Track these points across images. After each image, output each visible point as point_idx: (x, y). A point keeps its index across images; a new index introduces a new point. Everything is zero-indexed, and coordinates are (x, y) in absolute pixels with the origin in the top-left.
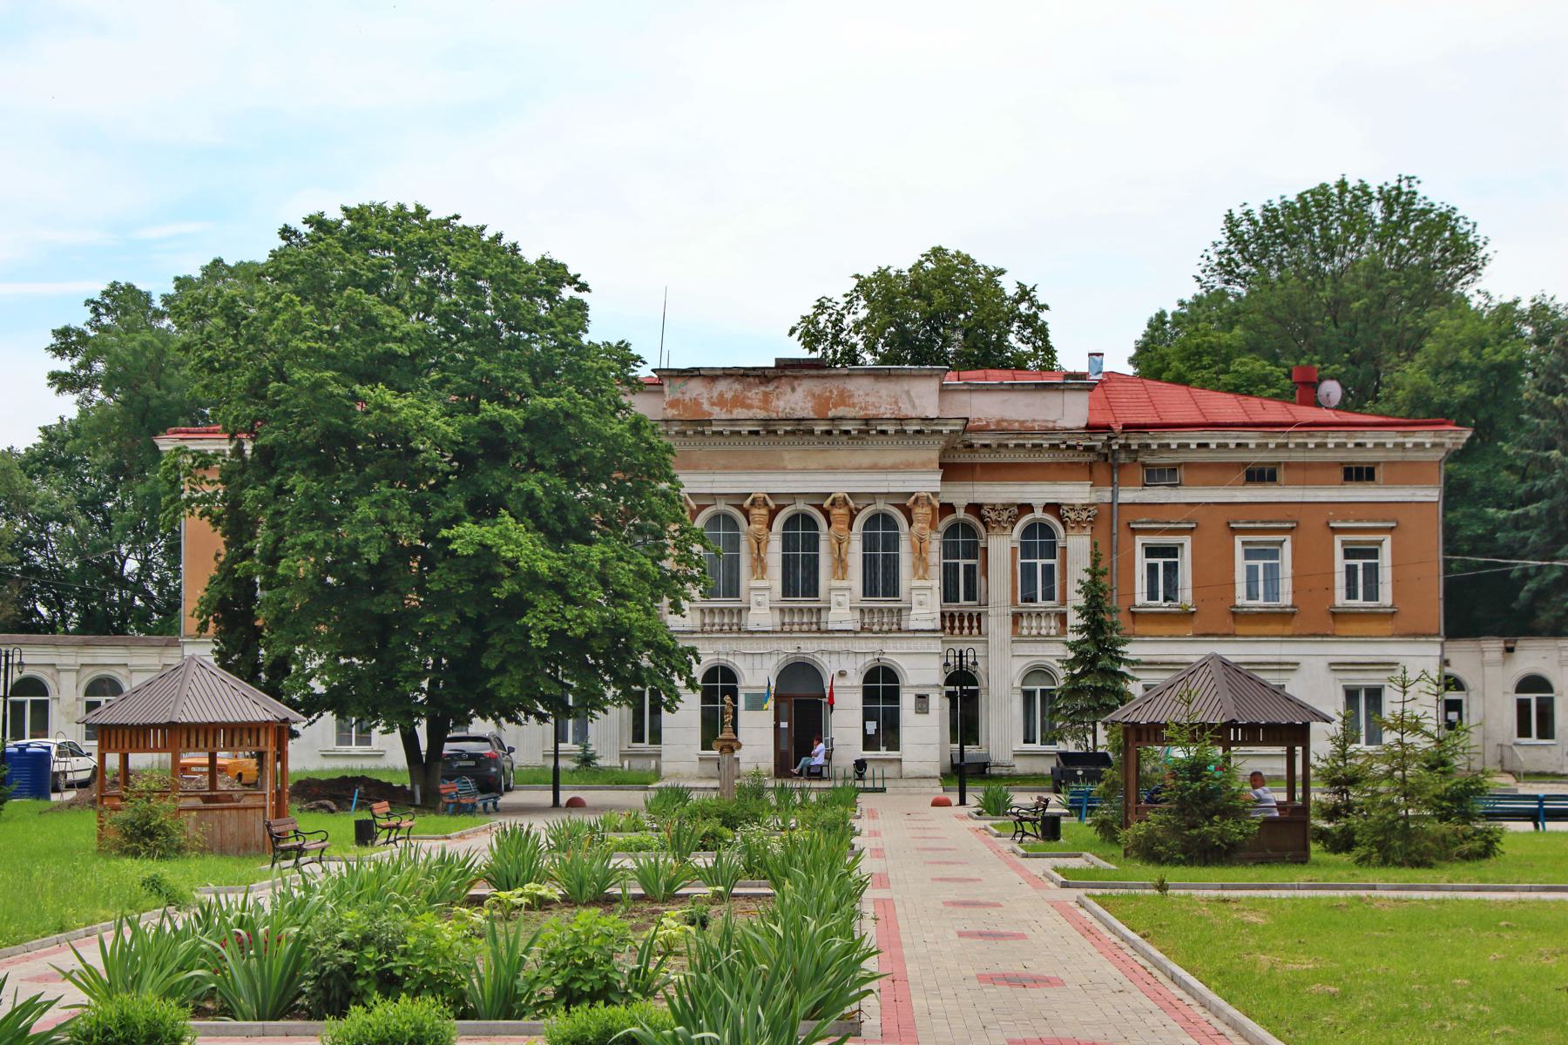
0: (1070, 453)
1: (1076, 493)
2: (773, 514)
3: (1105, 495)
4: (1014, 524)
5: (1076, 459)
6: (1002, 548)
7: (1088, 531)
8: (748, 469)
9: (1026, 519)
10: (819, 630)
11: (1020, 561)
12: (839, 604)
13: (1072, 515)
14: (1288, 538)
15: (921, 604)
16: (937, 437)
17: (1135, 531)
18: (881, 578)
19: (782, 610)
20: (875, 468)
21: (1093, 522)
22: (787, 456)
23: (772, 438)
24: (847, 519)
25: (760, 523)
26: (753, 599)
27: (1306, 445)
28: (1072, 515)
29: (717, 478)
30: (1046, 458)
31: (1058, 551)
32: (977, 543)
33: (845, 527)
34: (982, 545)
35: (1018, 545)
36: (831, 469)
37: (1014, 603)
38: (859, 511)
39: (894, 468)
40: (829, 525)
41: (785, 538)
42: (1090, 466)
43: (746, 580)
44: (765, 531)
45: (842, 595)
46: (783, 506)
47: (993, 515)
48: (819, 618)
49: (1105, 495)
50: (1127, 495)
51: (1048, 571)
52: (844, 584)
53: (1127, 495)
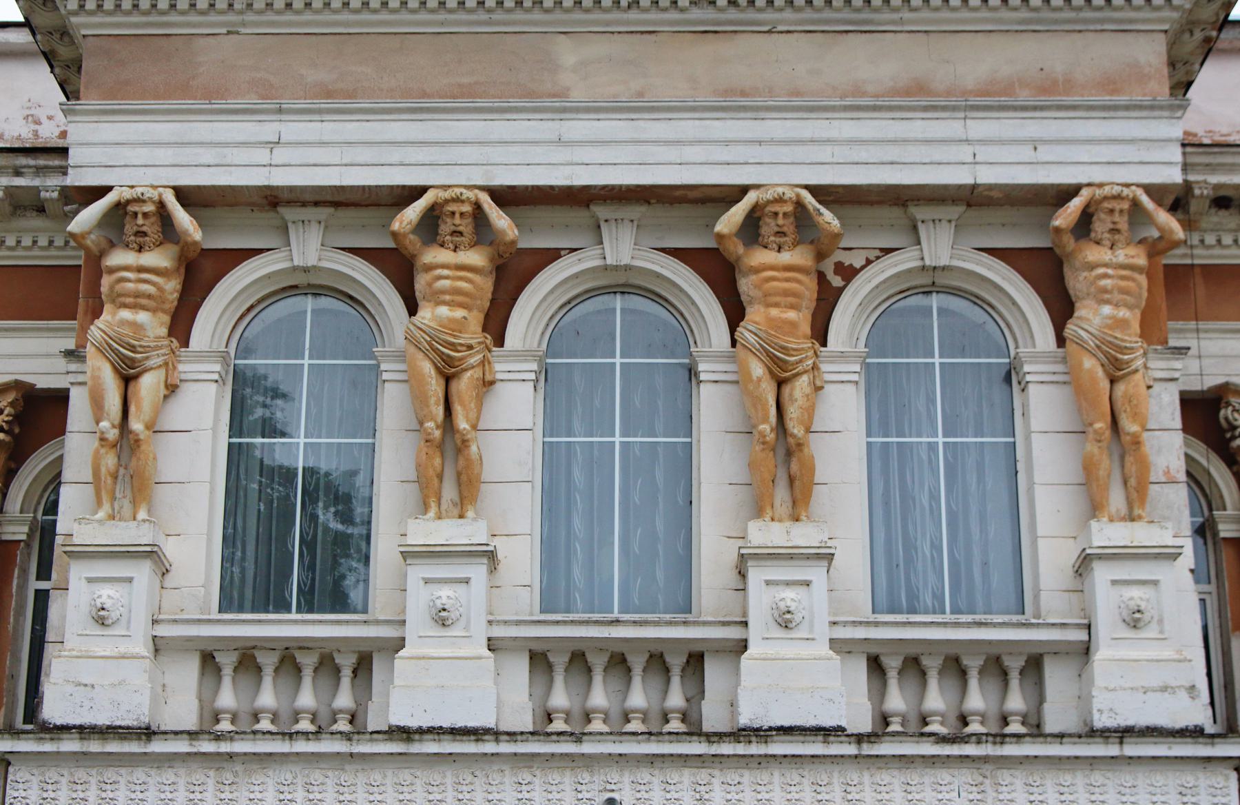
2: (512, 273)
8: (419, 101)
10: (695, 731)
12: (785, 621)
15: (1135, 620)
19: (539, 659)
20: (917, 97)
22: (568, 54)
24: (808, 288)
25: (458, 298)
26: (418, 601)
29: (293, 129)
33: (801, 318)
36: (736, 101)
38: (849, 273)
39: (993, 99)
40: (735, 313)
44: (473, 333)
46: (553, 255)
48: (697, 693)
52: (804, 536)
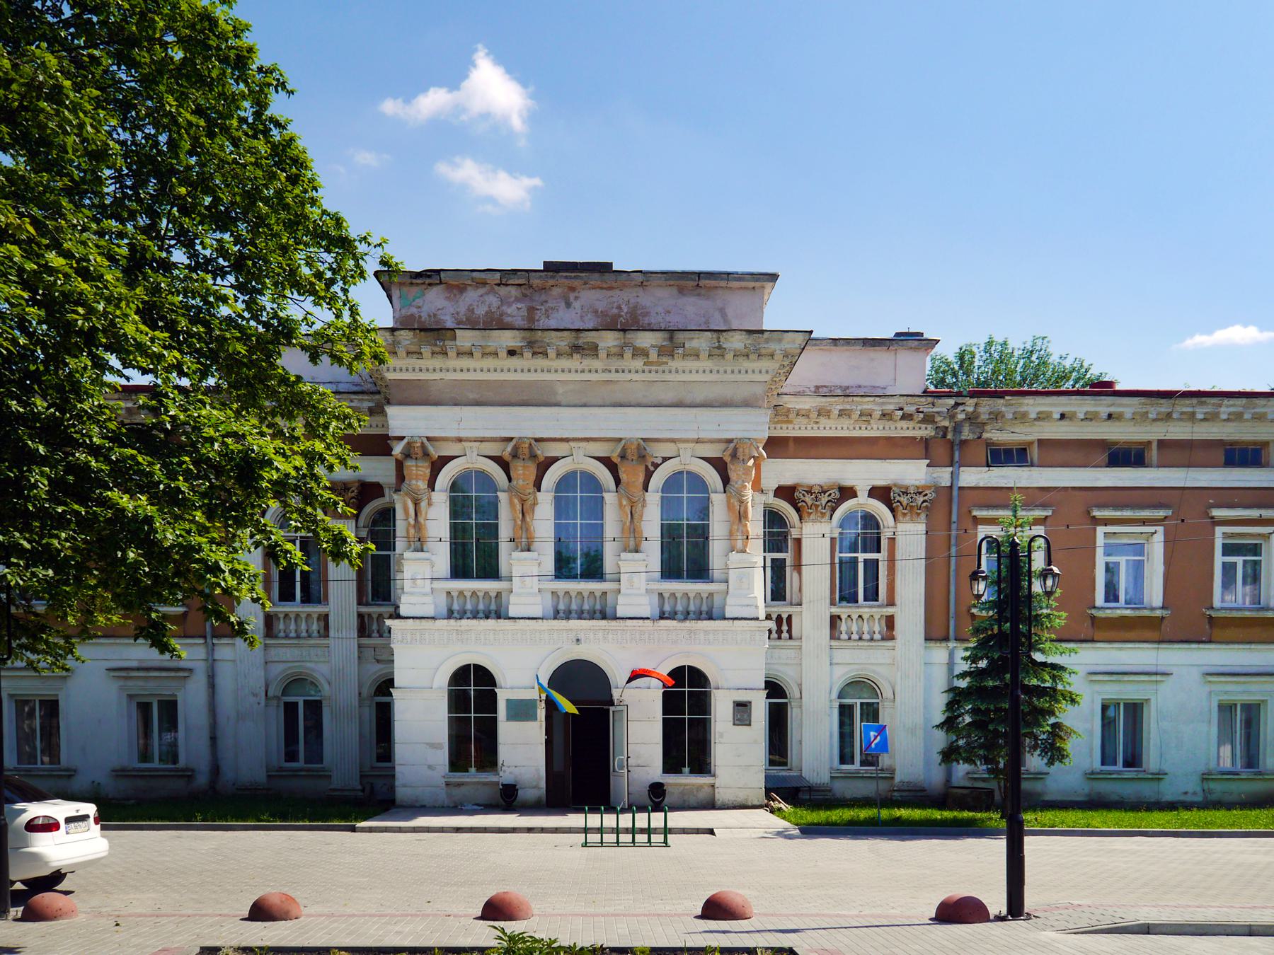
0: (904, 424)
1: (911, 473)
3: (943, 476)
4: (833, 510)
5: (910, 433)
6: (817, 538)
7: (923, 516)
9: (849, 505)
11: (838, 555)
13: (904, 500)
14: (1160, 529)
16: (765, 364)
17: (977, 521)
18: (686, 556)
21: (929, 510)
23: (540, 362)
27: (1193, 414)
28: (904, 500)
30: (875, 430)
31: (884, 543)
32: (785, 536)
34: (794, 533)
35: (836, 535)
37: (833, 603)
38: (656, 466)
41: (558, 502)
42: (926, 442)
43: (509, 558)
44: (531, 489)
45: (636, 577)
47: (808, 499)
49: (943, 476)
50: (972, 477)
51: (872, 566)
53: (972, 477)
